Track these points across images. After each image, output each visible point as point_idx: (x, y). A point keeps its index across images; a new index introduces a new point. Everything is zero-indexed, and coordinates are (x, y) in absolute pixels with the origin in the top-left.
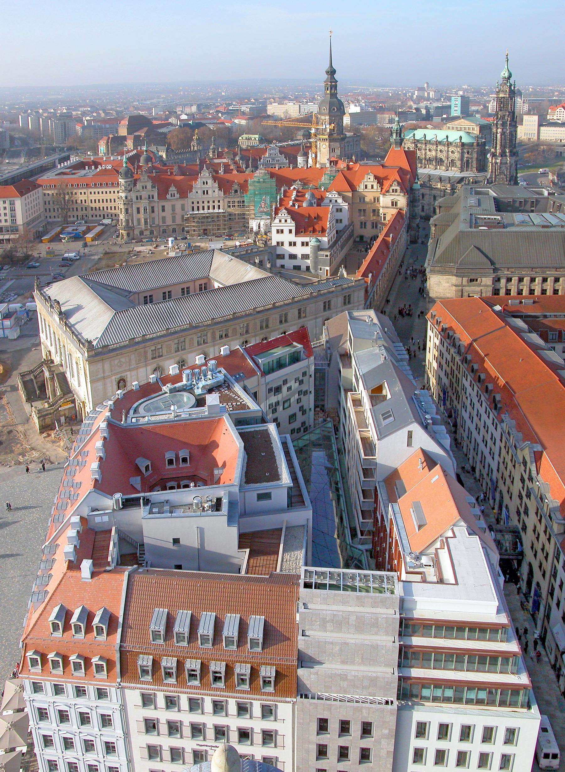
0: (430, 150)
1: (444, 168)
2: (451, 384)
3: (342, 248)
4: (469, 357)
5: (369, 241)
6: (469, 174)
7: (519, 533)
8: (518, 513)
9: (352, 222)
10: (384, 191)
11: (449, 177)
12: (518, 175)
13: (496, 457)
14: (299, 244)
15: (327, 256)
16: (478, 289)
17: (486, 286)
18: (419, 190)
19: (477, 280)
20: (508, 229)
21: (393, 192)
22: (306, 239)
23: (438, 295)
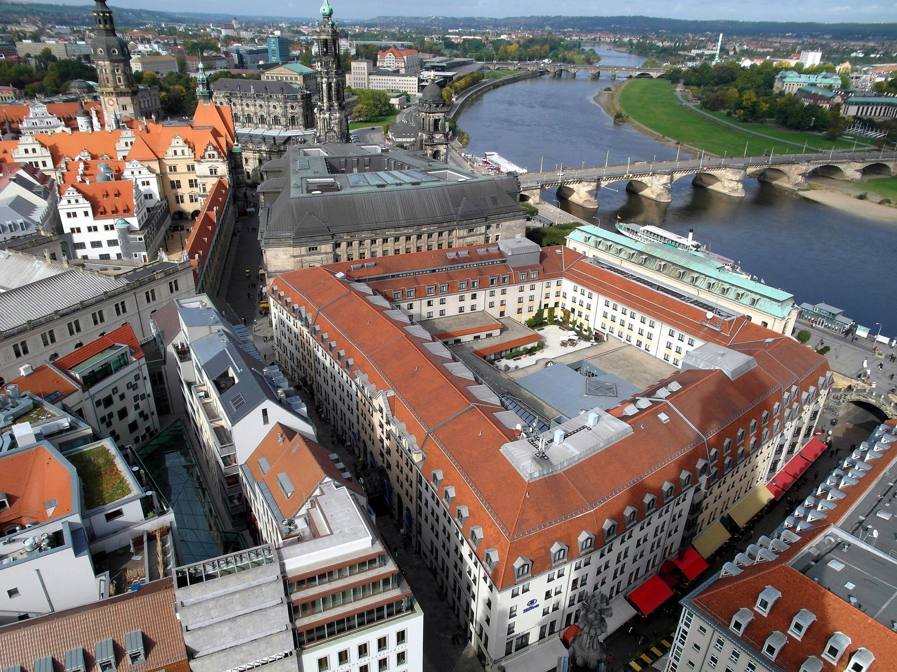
0: (248, 105)
1: (266, 126)
2: (304, 358)
3: (158, 229)
4: (318, 328)
5: (190, 217)
6: (296, 132)
7: (385, 471)
8: (382, 455)
9: (166, 197)
10: (198, 157)
11: (274, 138)
12: (351, 132)
13: (355, 411)
14: (101, 228)
15: (140, 239)
16: (318, 257)
17: (326, 253)
19: (316, 248)
20: (342, 192)
21: (210, 157)
22: (109, 222)
23: (277, 269)
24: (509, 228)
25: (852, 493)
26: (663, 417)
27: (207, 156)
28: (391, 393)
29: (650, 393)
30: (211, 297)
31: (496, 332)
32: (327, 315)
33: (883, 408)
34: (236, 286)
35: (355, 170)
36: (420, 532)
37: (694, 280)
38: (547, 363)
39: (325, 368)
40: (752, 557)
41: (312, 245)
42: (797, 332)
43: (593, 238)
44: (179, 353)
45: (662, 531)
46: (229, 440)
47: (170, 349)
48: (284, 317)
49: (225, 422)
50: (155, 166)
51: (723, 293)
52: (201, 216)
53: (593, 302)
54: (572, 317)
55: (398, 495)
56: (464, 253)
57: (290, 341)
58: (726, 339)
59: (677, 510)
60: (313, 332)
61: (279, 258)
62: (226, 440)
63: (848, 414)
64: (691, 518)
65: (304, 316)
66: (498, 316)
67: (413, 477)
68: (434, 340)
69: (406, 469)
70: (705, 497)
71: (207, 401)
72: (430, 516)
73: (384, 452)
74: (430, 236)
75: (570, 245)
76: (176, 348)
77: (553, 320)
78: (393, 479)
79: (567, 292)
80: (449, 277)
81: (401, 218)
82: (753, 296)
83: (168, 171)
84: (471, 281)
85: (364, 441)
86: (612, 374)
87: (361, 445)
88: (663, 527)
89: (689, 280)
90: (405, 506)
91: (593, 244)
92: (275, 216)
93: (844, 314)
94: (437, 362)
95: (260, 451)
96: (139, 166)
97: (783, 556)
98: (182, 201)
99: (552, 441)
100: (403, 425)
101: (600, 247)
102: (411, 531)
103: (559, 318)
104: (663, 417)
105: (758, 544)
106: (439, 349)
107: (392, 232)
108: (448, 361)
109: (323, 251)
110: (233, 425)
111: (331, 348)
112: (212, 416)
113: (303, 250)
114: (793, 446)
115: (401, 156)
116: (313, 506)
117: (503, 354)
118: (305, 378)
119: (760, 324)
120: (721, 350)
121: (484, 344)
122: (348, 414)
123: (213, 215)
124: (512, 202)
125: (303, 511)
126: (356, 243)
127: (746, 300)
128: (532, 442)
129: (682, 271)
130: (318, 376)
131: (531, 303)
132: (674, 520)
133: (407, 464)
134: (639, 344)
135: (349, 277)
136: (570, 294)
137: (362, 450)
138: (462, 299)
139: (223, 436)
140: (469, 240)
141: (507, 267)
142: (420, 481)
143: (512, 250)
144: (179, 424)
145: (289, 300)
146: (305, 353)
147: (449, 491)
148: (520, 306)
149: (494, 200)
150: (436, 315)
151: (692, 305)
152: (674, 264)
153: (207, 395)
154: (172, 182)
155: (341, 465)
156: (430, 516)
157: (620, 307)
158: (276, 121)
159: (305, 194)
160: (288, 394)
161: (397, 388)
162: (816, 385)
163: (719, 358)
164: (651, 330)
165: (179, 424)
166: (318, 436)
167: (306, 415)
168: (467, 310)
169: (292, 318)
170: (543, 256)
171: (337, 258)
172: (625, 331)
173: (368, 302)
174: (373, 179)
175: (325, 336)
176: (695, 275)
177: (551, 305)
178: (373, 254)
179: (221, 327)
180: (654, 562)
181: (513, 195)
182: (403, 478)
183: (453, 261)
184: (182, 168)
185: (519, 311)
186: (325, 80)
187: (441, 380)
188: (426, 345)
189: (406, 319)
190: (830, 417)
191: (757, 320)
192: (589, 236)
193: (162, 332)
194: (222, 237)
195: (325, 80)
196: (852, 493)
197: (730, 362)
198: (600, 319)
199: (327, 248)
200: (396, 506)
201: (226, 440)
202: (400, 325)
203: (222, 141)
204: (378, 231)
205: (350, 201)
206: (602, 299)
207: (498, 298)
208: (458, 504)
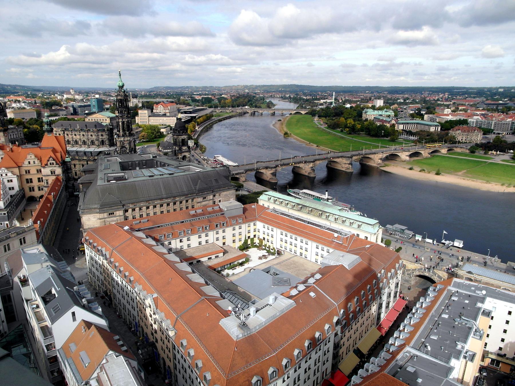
0: (75, 135)
4: (112, 260)
9: (23, 188)
10: (43, 165)
11: (91, 152)
15: (5, 214)
16: (115, 219)
17: (120, 216)
18: (70, 162)
19: (113, 213)
23: (89, 227)
24: (226, 195)
25: (417, 326)
26: (312, 294)
27: (49, 164)
28: (155, 295)
29: (305, 282)
30: (45, 247)
31: (221, 255)
32: (119, 252)
33: (432, 278)
34: (63, 239)
35: (138, 168)
36: (177, 381)
37: (327, 217)
38: (250, 270)
39: (117, 284)
40: (367, 370)
41: (111, 212)
42: (384, 240)
43: (272, 198)
44: (21, 282)
45: (319, 362)
46: (51, 334)
47: (16, 279)
48: (93, 255)
49: (48, 323)
50: (16, 170)
51: (343, 223)
52: (44, 198)
53: (274, 233)
54: (264, 243)
55: (163, 359)
56: (199, 211)
57: (97, 269)
58: (346, 247)
59: (326, 348)
60: (110, 263)
61: (90, 220)
62: (48, 334)
63: (416, 283)
64: (335, 352)
65: (104, 254)
66: (222, 245)
67: (170, 346)
68: (182, 262)
69: (166, 341)
70: (342, 339)
71: (38, 310)
72: (181, 369)
73: (153, 332)
74: (181, 202)
75: (261, 203)
76: (20, 278)
77: (254, 245)
78: (159, 348)
79: (259, 229)
80: (192, 225)
81: (163, 194)
82: (358, 223)
83: (25, 173)
84: (205, 226)
85: (142, 327)
86: (286, 272)
87: (141, 329)
88: (319, 359)
89: (325, 217)
90: (167, 365)
91: (273, 202)
92: (88, 196)
93: (408, 229)
94: (183, 275)
95: (71, 339)
96: (6, 171)
97: (383, 368)
98: (33, 190)
99: (249, 314)
100: (163, 314)
101: (277, 203)
102: (171, 381)
103: (257, 244)
104: (312, 294)
105: (371, 362)
106: (185, 267)
107: (159, 202)
108: (189, 273)
109: (117, 215)
110: (52, 324)
111: (120, 271)
112: (40, 319)
113: (106, 215)
114: (388, 303)
115: (164, 159)
116: (101, 371)
117: (226, 267)
118: (106, 291)
119: (363, 238)
120: (342, 253)
121: (214, 262)
122: (132, 310)
123: (51, 197)
124: (227, 182)
125: (95, 375)
126: (137, 209)
127: (355, 226)
128: (238, 317)
129: (321, 213)
130: (113, 289)
131: (240, 237)
132: (325, 354)
133: (166, 338)
134: (301, 254)
135: (132, 229)
136: (262, 230)
137: (141, 333)
138: (200, 237)
139: (46, 331)
140: (204, 203)
141: (225, 217)
142: (174, 348)
143: (227, 207)
144: (21, 327)
145: (95, 244)
146: (106, 276)
147: (190, 352)
148: (234, 238)
149: (216, 180)
150: (185, 248)
151: (326, 230)
152: (316, 209)
153: (38, 307)
154: (27, 180)
155: (121, 343)
156: (181, 369)
157: (289, 235)
158: (93, 143)
159: (106, 183)
160: (89, 302)
161: (158, 292)
162: (395, 269)
163: (341, 258)
164: (306, 246)
165: (21, 327)
166: (110, 328)
167: (101, 313)
168: (204, 243)
169: (97, 255)
170: (245, 210)
171: (126, 218)
172: (293, 248)
173: (143, 242)
174: (146, 172)
175: (117, 264)
176: (328, 214)
177: (252, 237)
178: (148, 215)
179: (49, 263)
180: (317, 382)
181: (227, 177)
182: (165, 347)
183: (194, 216)
184: (33, 171)
185: (234, 241)
186: (120, 120)
187: (185, 285)
188: (176, 265)
189: (165, 251)
190: (407, 285)
191: (362, 236)
192: (270, 197)
193: (12, 270)
194: (57, 210)
195: (120, 120)
196: (417, 326)
197: (348, 261)
198: (279, 243)
199: (120, 213)
200: (162, 366)
201: (48, 334)
202: (161, 255)
203: (59, 155)
204: (150, 202)
205: (133, 187)
206: (279, 231)
207: (221, 235)
208: (196, 360)
